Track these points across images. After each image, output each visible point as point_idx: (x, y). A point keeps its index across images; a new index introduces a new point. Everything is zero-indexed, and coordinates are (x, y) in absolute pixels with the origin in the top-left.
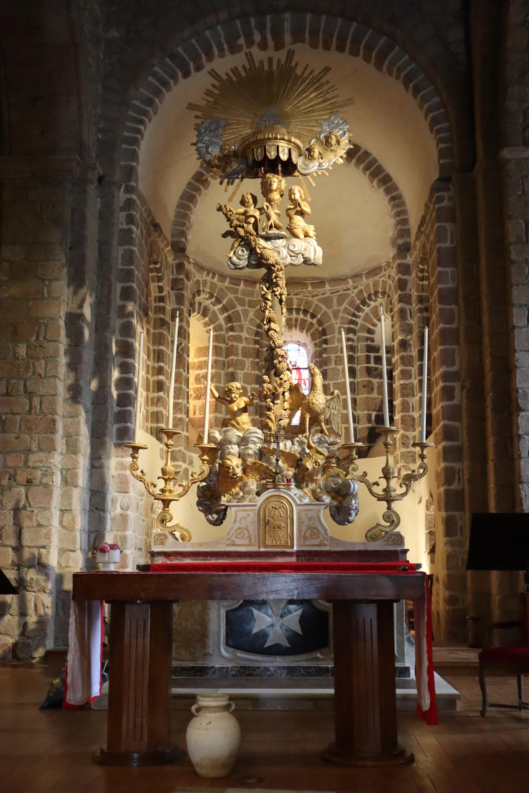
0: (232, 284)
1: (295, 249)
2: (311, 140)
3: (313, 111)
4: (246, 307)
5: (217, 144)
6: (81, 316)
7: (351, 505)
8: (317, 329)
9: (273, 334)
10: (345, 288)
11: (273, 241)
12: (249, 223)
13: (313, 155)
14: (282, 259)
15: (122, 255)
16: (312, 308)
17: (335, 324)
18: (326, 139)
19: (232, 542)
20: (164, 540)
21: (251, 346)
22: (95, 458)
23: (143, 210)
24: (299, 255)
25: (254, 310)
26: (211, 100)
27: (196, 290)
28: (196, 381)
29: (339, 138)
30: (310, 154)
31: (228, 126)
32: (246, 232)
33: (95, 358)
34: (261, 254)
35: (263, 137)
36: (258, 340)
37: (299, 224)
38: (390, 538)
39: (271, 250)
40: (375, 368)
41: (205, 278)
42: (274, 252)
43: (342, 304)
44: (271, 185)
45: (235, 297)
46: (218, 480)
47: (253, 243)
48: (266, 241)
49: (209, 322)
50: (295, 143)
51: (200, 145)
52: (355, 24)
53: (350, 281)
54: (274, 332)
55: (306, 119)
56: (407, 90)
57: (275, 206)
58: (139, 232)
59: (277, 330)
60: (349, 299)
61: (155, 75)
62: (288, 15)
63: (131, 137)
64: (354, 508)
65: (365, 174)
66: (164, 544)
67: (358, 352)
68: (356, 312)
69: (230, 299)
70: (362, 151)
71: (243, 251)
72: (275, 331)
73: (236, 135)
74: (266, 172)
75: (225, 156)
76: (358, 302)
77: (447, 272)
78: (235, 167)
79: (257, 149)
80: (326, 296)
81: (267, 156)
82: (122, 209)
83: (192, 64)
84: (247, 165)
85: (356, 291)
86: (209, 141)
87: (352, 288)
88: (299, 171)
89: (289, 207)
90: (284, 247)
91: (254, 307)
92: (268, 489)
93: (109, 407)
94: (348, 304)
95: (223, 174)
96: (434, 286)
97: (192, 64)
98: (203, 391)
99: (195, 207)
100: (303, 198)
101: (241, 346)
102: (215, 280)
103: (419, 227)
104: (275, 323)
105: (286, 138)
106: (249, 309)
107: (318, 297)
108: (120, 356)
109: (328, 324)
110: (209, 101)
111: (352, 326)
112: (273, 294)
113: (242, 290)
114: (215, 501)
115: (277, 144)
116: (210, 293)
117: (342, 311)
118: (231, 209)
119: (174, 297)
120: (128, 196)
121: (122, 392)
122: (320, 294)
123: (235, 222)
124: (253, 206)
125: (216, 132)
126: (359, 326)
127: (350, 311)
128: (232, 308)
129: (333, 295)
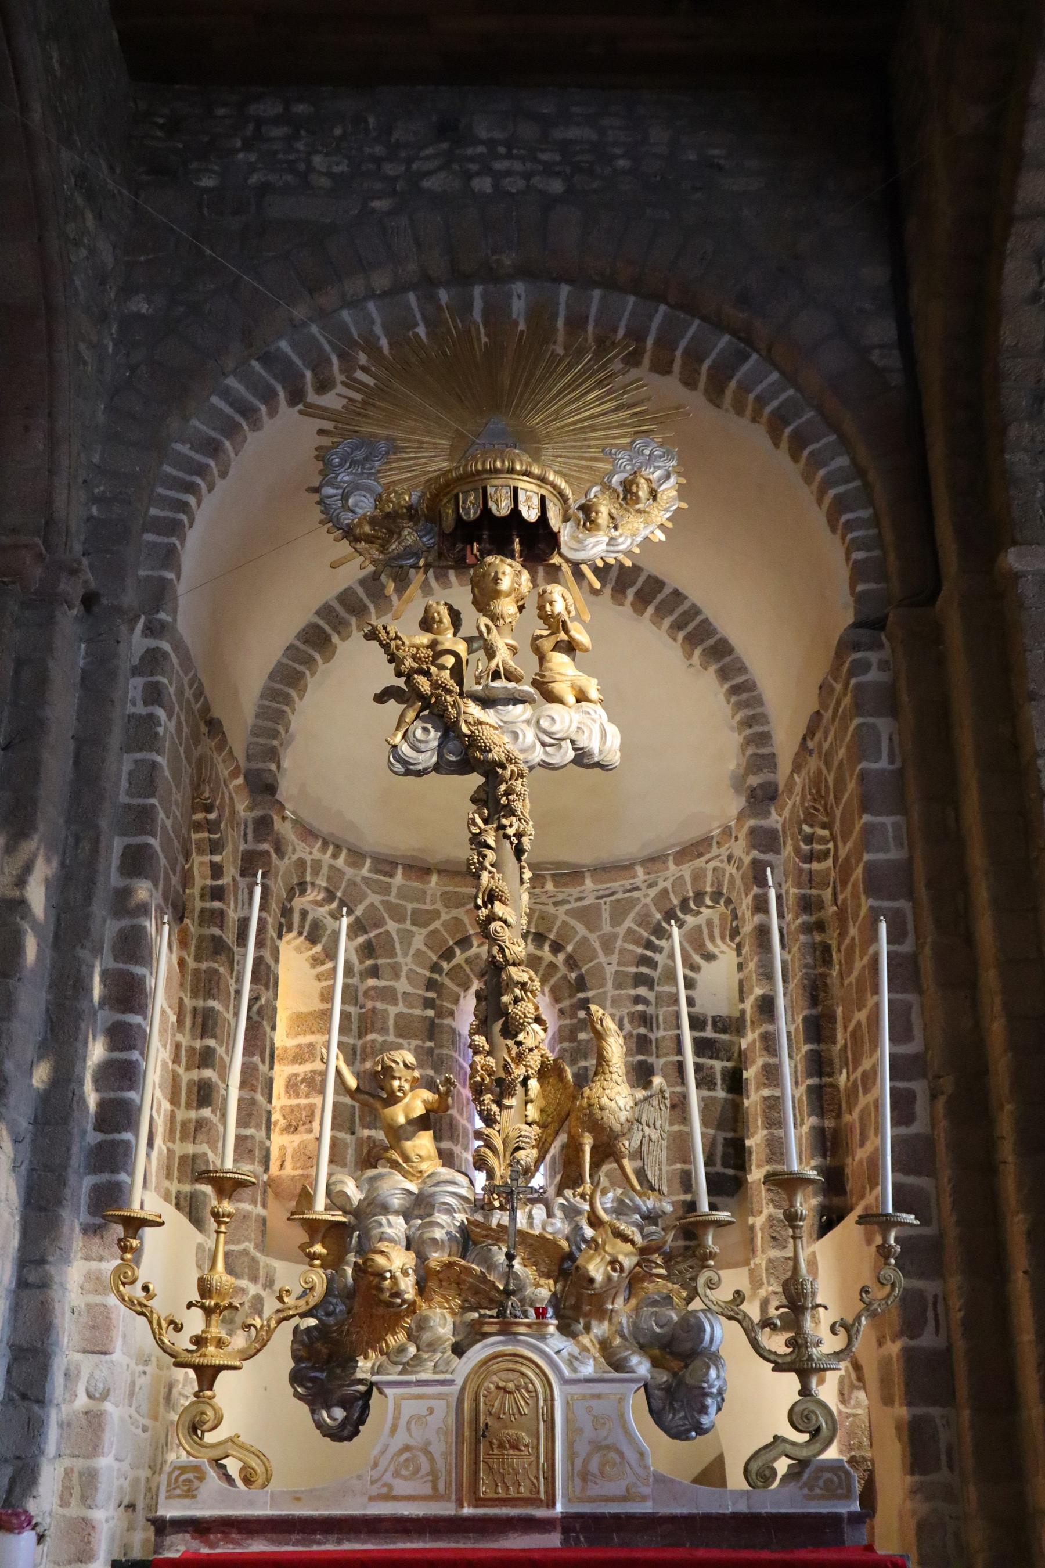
0: (378, 872)
1: (554, 729)
2: (590, 489)
3: (593, 428)
4: (408, 925)
5: (369, 489)
6: (21, 904)
7: (707, 1382)
8: (565, 978)
9: (499, 929)
10: (629, 887)
11: (499, 707)
12: (442, 667)
13: (596, 518)
14: (522, 751)
15: (130, 774)
16: (555, 930)
17: (605, 965)
18: (625, 487)
19: (385, 1490)
20: (196, 1483)
21: (417, 1012)
22: (32, 1262)
23: (186, 681)
24: (563, 743)
25: (425, 931)
26: (358, 397)
27: (295, 881)
28: (287, 1091)
29: (654, 486)
30: (588, 518)
31: (394, 453)
32: (435, 685)
33: (47, 1010)
34: (472, 736)
35: (480, 467)
36: (433, 999)
37: (562, 671)
38: (817, 1478)
39: (496, 729)
41: (317, 855)
42: (503, 733)
43: (623, 921)
44: (496, 580)
45: (382, 902)
46: (349, 1311)
47: (453, 712)
48: (483, 709)
49: (323, 956)
50: (554, 486)
51: (329, 491)
52: (663, 308)
53: (640, 870)
54: (500, 923)
55: (579, 443)
56: (777, 445)
57: (506, 630)
58: (172, 726)
59: (510, 920)
60: (637, 909)
61: (226, 394)
62: (519, 287)
63: (165, 518)
64: (714, 1391)
65: (675, 640)
66: (194, 1497)
67: (658, 1028)
68: (653, 938)
69: (372, 905)
70: (667, 591)
71: (425, 730)
72: (505, 922)
73: (414, 473)
74: (484, 553)
75: (388, 515)
76: (658, 916)
77: (883, 825)
78: (410, 540)
79: (466, 493)
80: (585, 903)
81: (490, 510)
82: (135, 671)
83: (309, 375)
84: (443, 535)
85: (653, 892)
86: (349, 483)
87: (643, 886)
88: (561, 555)
89: (538, 632)
90: (528, 722)
91: (425, 925)
92: (486, 1335)
93: (76, 1131)
94: (635, 921)
95: (381, 556)
96: (853, 861)
97: (309, 375)
98: (304, 1114)
99: (301, 698)
100: (573, 613)
101: (393, 1011)
102: (340, 862)
103: (804, 739)
104: (504, 903)
105: (536, 470)
106: (414, 928)
107: (568, 907)
108: (111, 1008)
109: (591, 964)
110: (351, 400)
111: (644, 970)
112: (501, 832)
113: (399, 888)
114: (338, 1371)
115: (513, 483)
116: (327, 890)
117: (621, 936)
118: (399, 634)
120: (152, 643)
121: (112, 1095)
122: (571, 899)
123: (409, 663)
124: (452, 631)
125: (368, 466)
126: (659, 969)
127: (641, 937)
128: (376, 926)
129: (602, 901)
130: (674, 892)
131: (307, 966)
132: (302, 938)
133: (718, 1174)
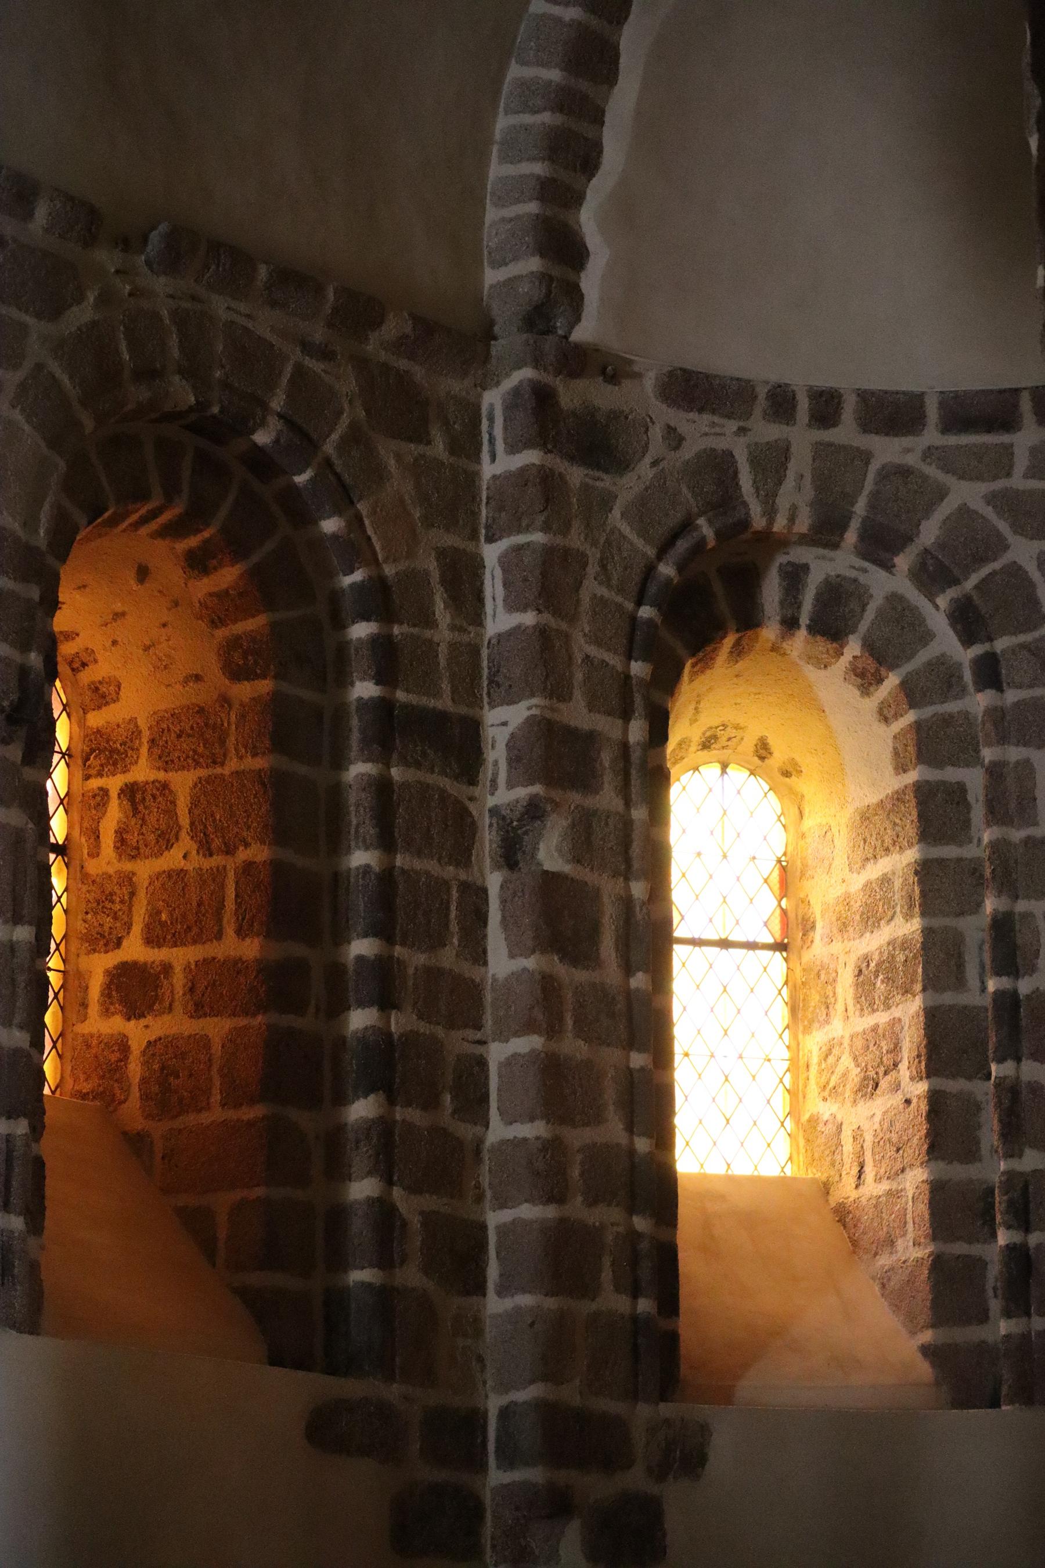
28: (857, 999)
45: (991, 499)
49: (871, 665)
119: (498, 573)
131: (851, 693)
132: (802, 633)
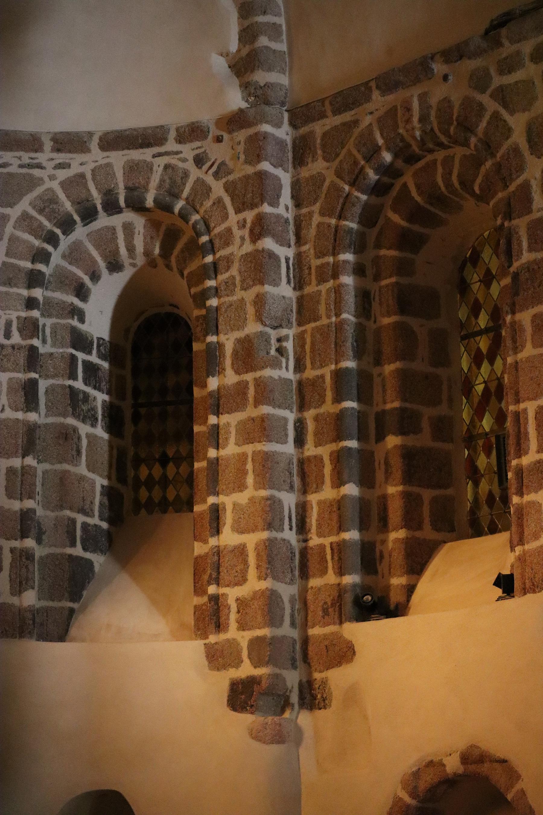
10: (28, 161)
40: (84, 393)
85: (62, 174)
127: (41, 226)
130: (94, 179)
133: (96, 525)
